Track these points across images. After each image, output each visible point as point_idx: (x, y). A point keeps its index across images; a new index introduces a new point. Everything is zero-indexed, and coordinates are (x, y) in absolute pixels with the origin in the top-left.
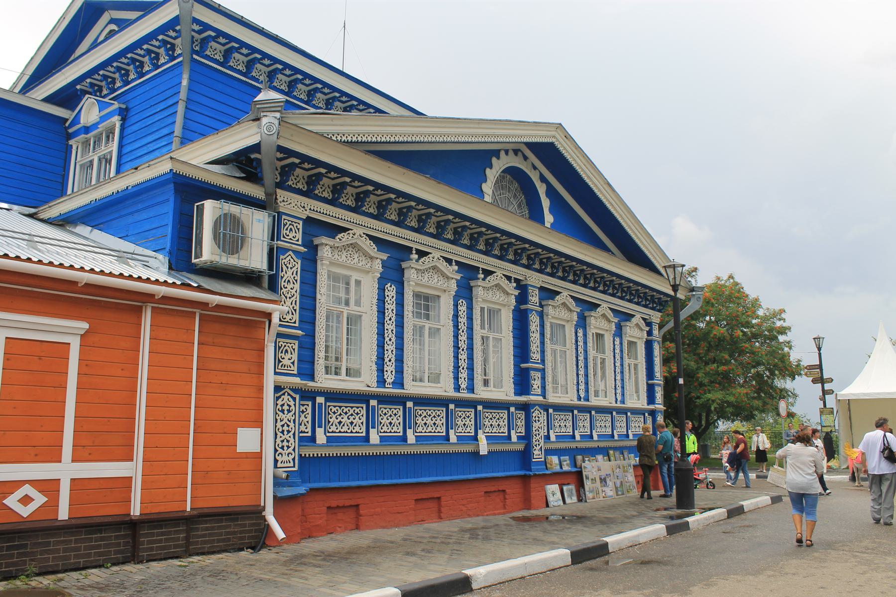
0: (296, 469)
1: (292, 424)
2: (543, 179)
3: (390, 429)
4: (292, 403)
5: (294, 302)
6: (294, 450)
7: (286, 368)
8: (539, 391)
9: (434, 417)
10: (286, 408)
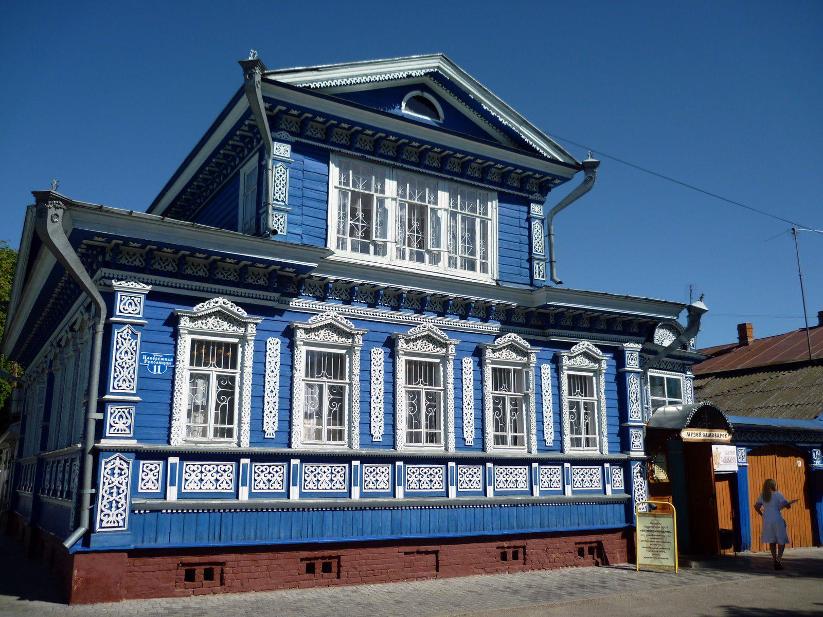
4: (125, 466)
7: (120, 432)
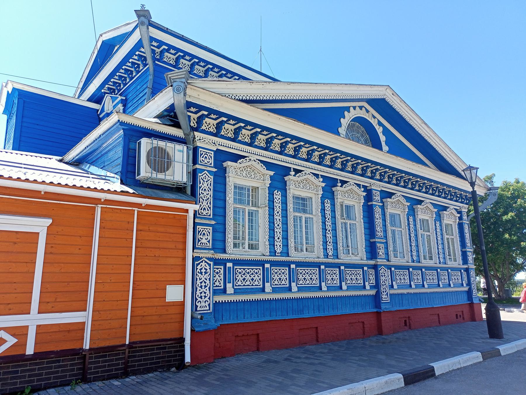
1: (208, 282)
2: (380, 124)
4: (208, 267)
5: (209, 203)
6: (209, 298)
7: (204, 245)
8: (384, 257)
9: (311, 274)
10: (203, 271)
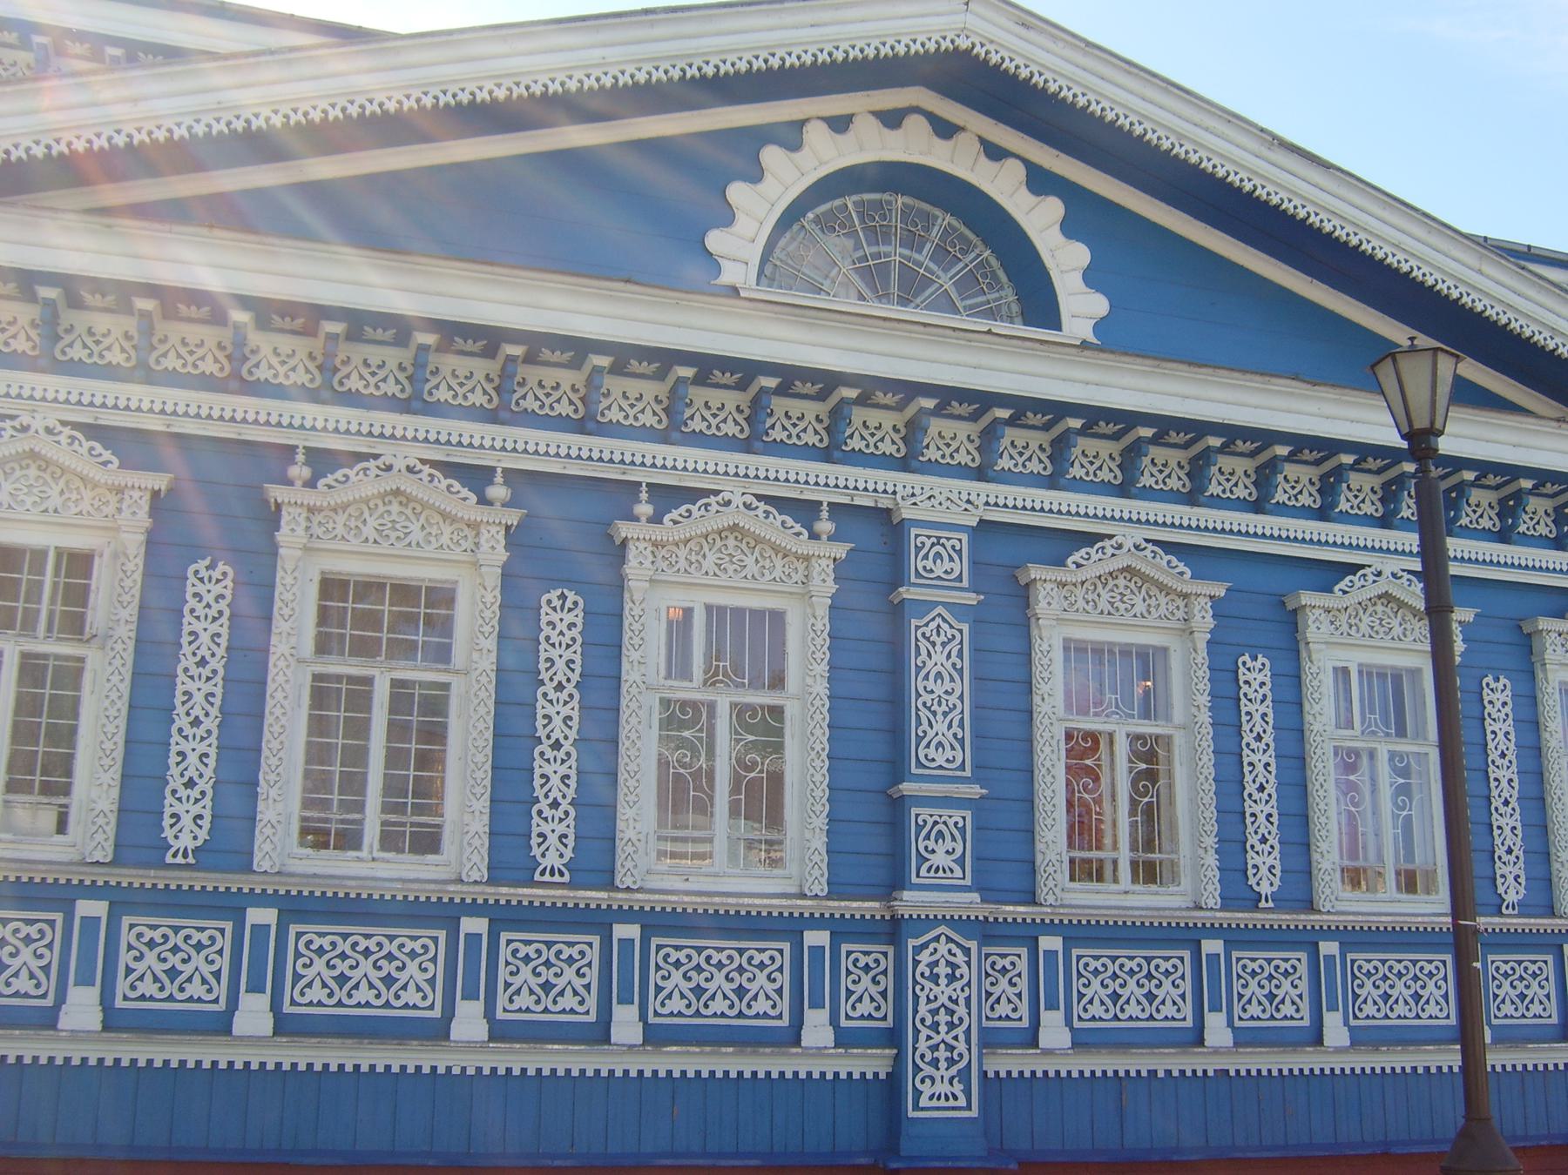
0: (974, 1113)
3: (1522, 1009)
4: (960, 958)
5: (956, 723)
10: (943, 970)
